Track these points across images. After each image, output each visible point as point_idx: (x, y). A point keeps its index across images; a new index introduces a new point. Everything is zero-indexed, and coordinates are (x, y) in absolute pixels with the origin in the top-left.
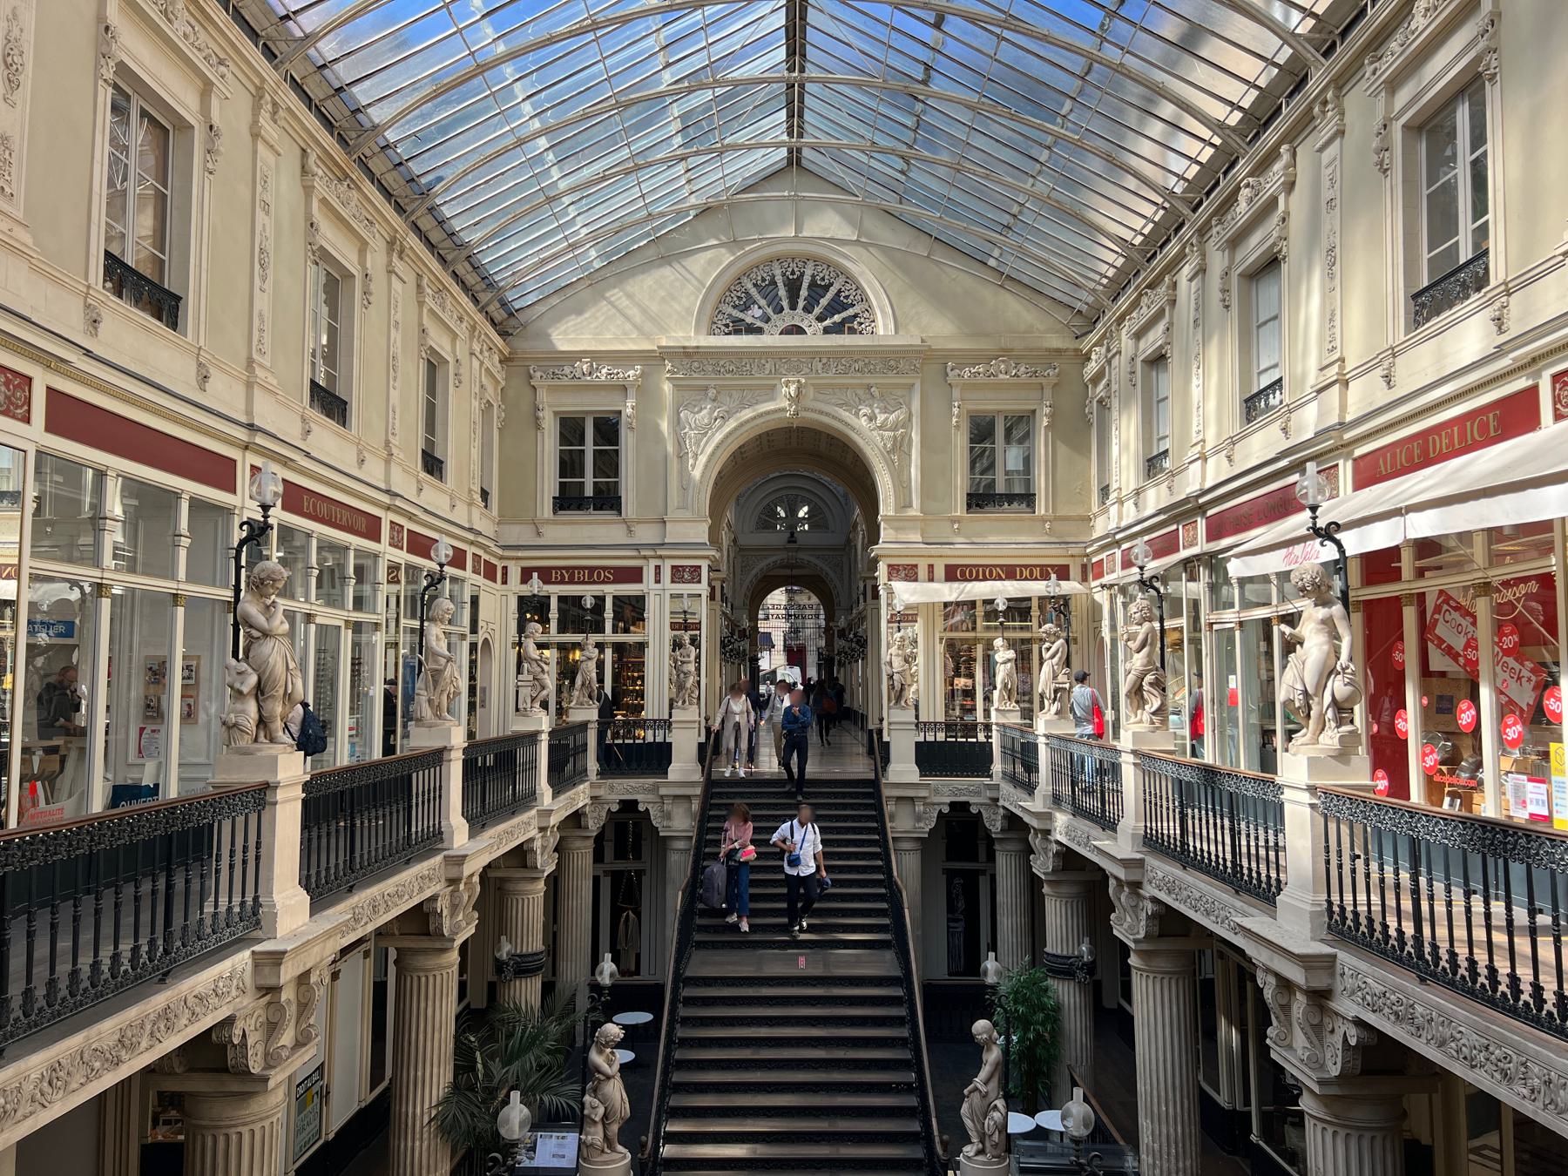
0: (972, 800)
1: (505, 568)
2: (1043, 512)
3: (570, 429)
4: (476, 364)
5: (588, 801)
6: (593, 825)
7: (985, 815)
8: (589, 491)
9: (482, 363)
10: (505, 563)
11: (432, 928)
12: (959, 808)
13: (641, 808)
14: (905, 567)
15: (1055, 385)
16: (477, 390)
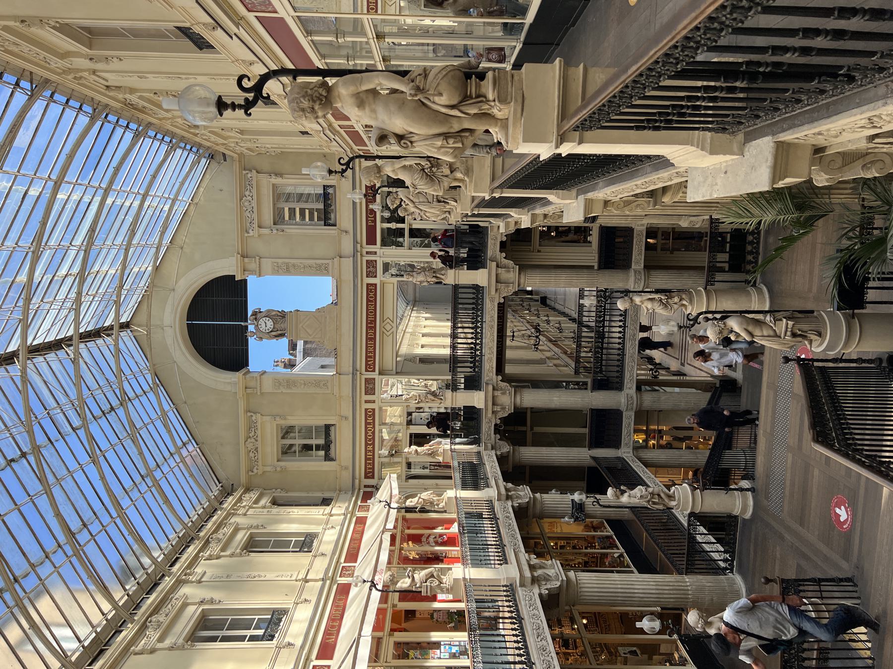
0: (499, 240)
1: (365, 486)
2: (334, 181)
3: (287, 451)
4: (251, 512)
5: (493, 452)
6: (506, 448)
7: (505, 295)
8: (321, 441)
9: (251, 507)
10: (362, 486)
11: (556, 592)
12: (503, 245)
13: (498, 422)
14: (368, 267)
15: (258, 172)
16: (265, 510)
